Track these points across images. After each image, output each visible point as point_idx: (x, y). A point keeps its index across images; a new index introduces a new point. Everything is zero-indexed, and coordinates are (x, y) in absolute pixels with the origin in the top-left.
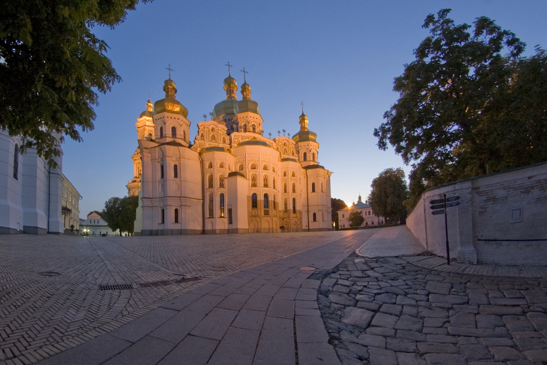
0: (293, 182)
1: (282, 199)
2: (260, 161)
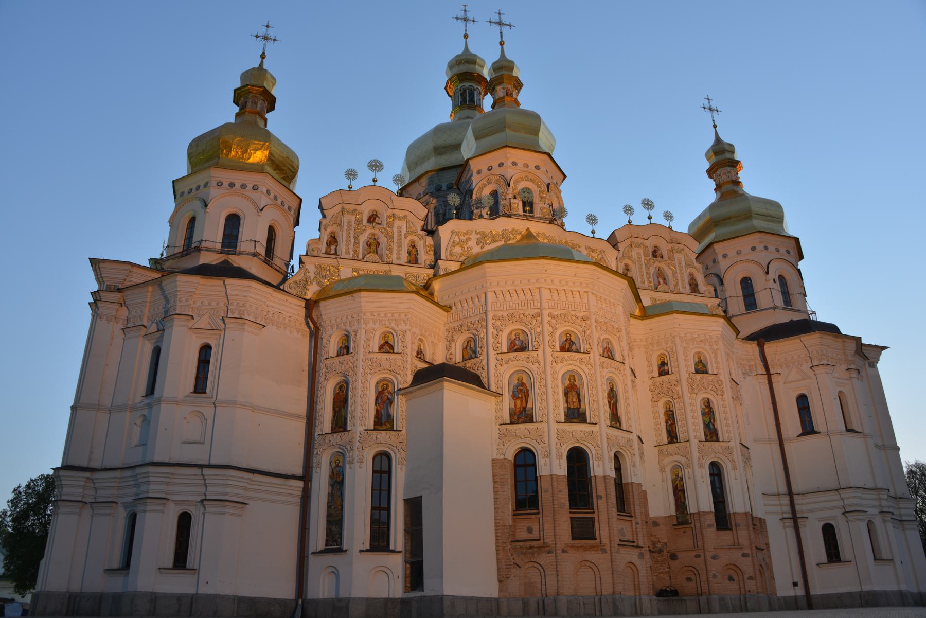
0: (702, 395)
1: (662, 470)
2: (546, 318)
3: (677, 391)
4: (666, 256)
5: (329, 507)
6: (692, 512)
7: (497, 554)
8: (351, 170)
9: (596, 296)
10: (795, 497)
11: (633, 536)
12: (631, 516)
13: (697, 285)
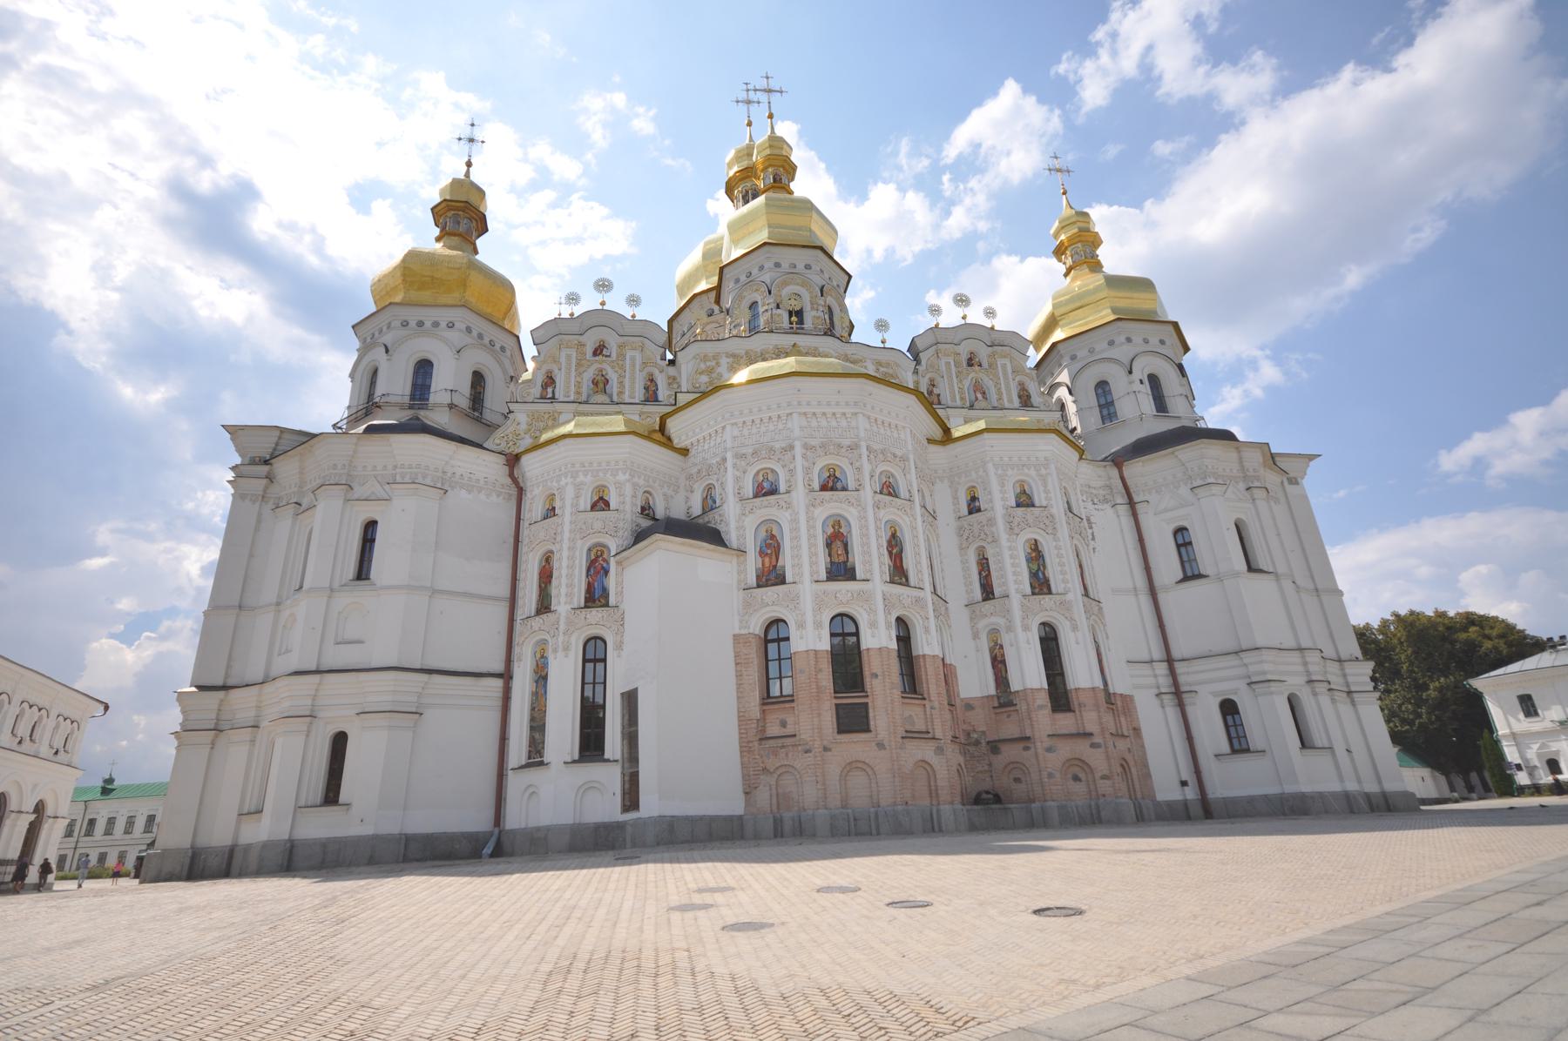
1: (976, 636)
2: (798, 450)
3: (993, 533)
4: (985, 365)
5: (533, 709)
6: (1016, 689)
7: (742, 757)
8: (572, 294)
9: (869, 418)
10: (1177, 665)
11: (927, 726)
12: (924, 699)
13: (1029, 397)
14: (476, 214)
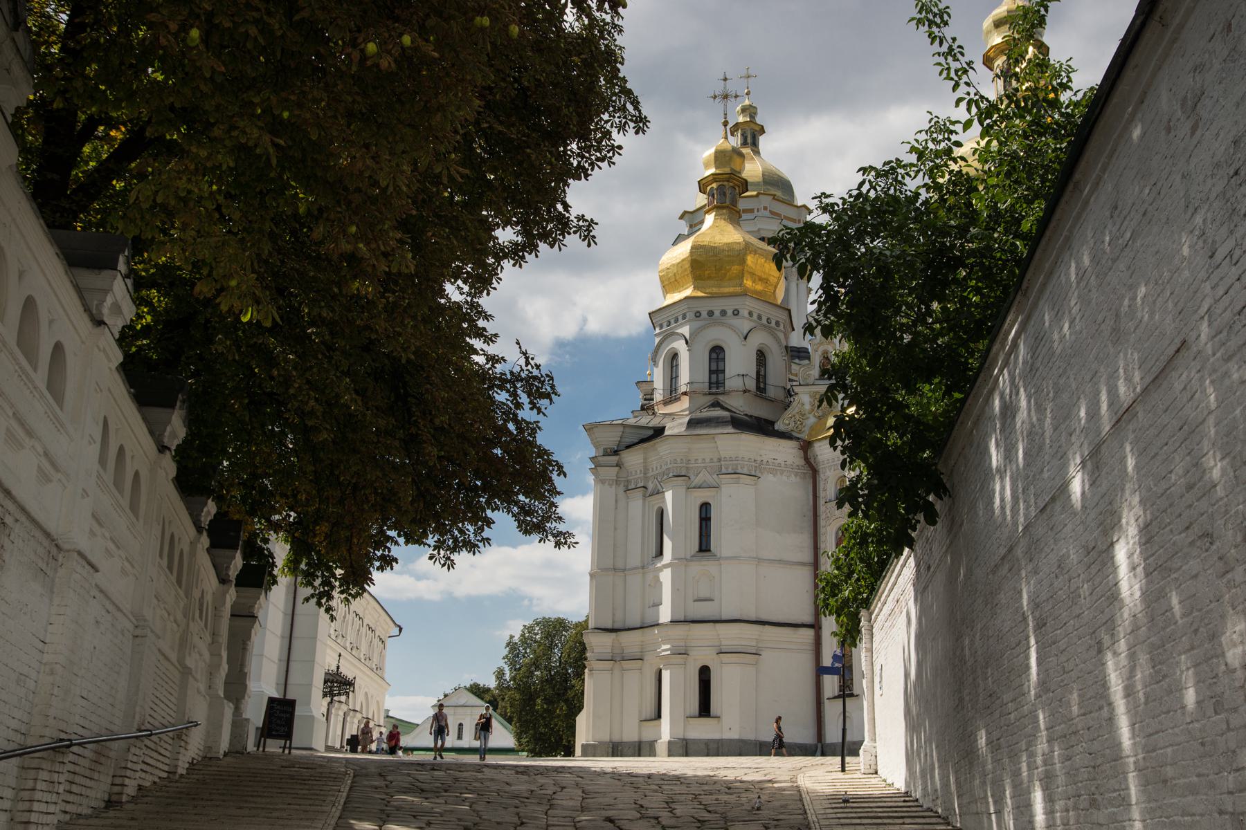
14: (740, 182)
